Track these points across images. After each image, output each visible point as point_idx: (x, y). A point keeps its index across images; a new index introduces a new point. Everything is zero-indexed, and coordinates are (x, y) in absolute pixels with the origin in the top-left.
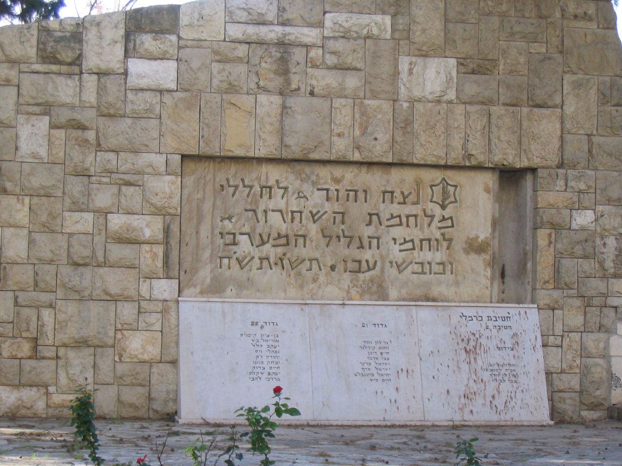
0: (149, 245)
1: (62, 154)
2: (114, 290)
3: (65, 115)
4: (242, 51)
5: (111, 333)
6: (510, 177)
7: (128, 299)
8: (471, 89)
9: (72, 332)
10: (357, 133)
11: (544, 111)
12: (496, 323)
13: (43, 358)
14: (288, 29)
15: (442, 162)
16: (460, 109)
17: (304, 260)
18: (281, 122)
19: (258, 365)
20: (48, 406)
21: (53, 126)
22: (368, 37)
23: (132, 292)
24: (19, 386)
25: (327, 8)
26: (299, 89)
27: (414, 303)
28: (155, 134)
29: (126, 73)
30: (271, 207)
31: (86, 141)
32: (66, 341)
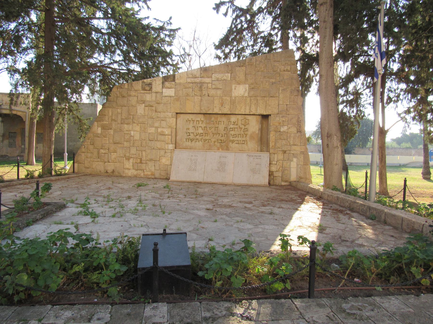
2: (159, 147)
3: (147, 104)
7: (163, 149)
8: (252, 93)
14: (203, 79)
15: (244, 113)
21: (145, 106)
24: (137, 170)
25: (213, 72)
27: (27, 139)
29: (162, 92)
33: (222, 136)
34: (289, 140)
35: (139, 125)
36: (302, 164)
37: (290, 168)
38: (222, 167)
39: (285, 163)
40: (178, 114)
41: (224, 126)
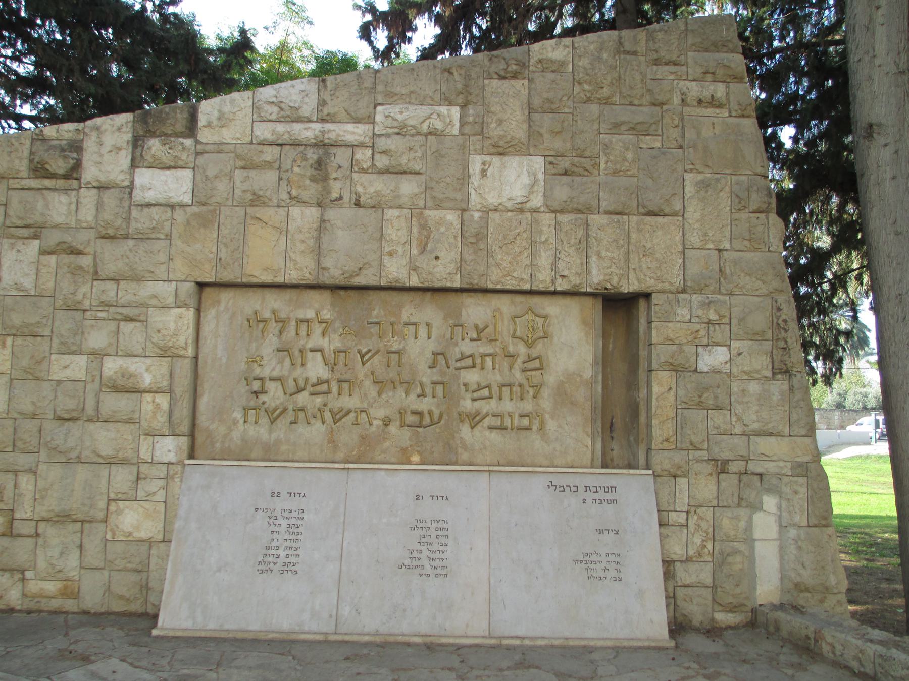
0: (152, 394)
1: (51, 285)
2: (106, 450)
3: (53, 238)
4: (270, 154)
5: (102, 504)
6: (620, 308)
7: (125, 462)
9: (52, 504)
10: (415, 251)
11: (660, 219)
12: (597, 496)
13: (19, 536)
14: (328, 126)
15: (527, 287)
16: (547, 219)
17: (349, 412)
18: (318, 239)
19: (272, 552)
20: (24, 595)
21: (43, 252)
22: (430, 133)
23: (130, 454)
25: (380, 99)
26: (341, 198)
28: (162, 257)
29: (131, 187)
30: (310, 345)
31: (81, 268)
32: (45, 514)
33: (422, 395)
34: (738, 409)
35: (9, 341)
36: (805, 523)
37: (750, 541)
38: (427, 552)
39: (726, 522)
40: (208, 290)
41: (432, 346)
